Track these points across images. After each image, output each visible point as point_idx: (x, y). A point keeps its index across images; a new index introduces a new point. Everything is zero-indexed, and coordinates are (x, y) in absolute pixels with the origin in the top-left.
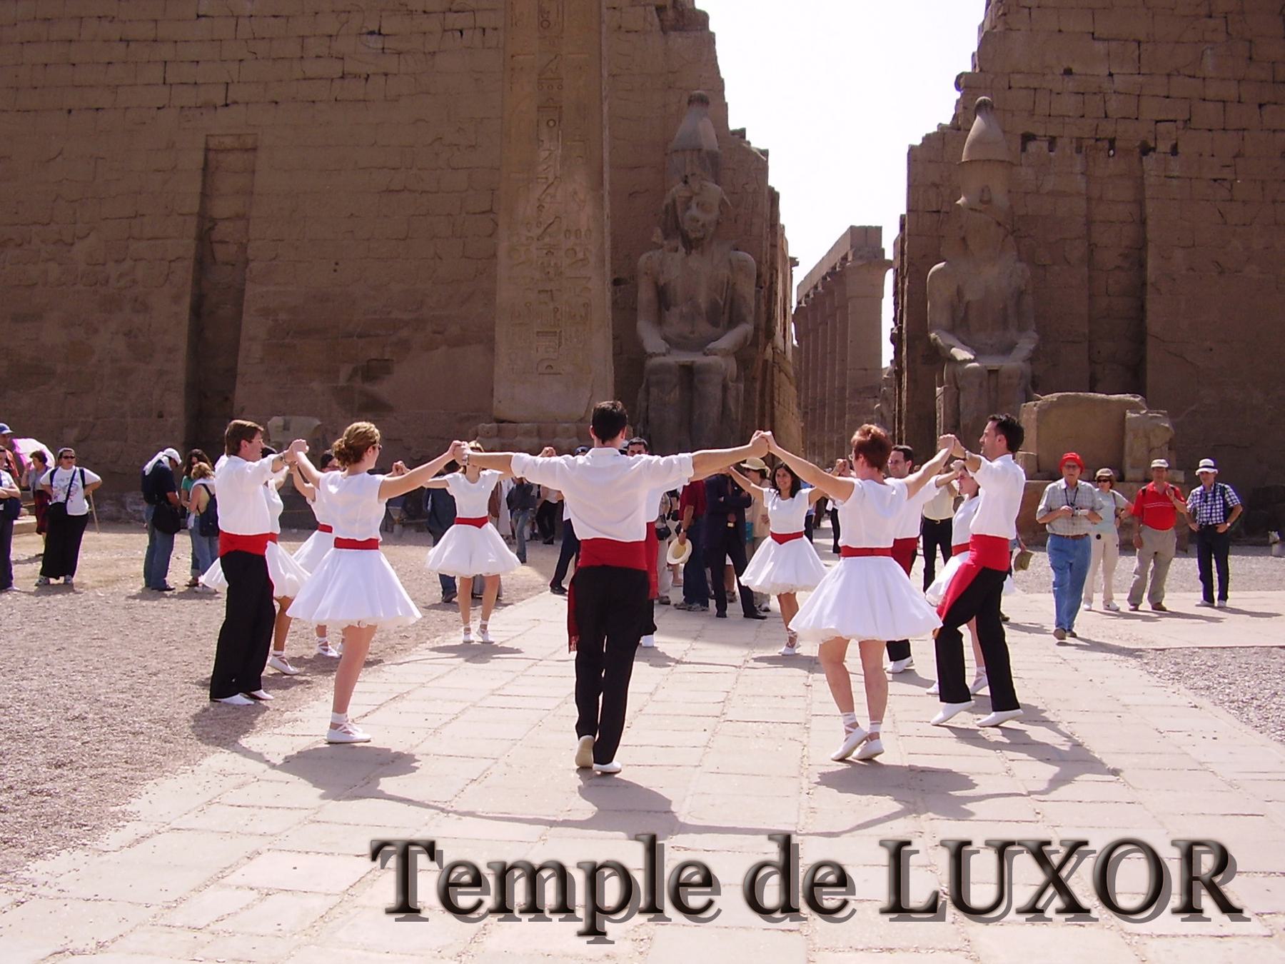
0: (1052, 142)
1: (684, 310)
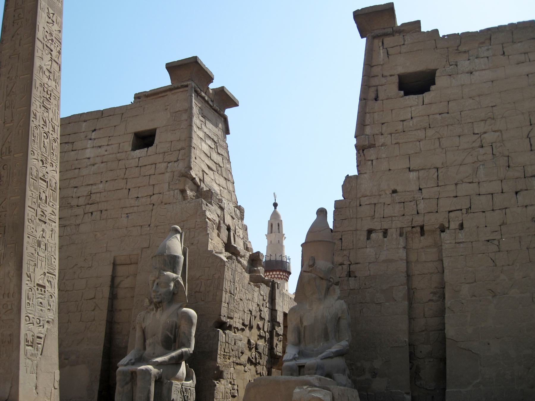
0: (385, 233)
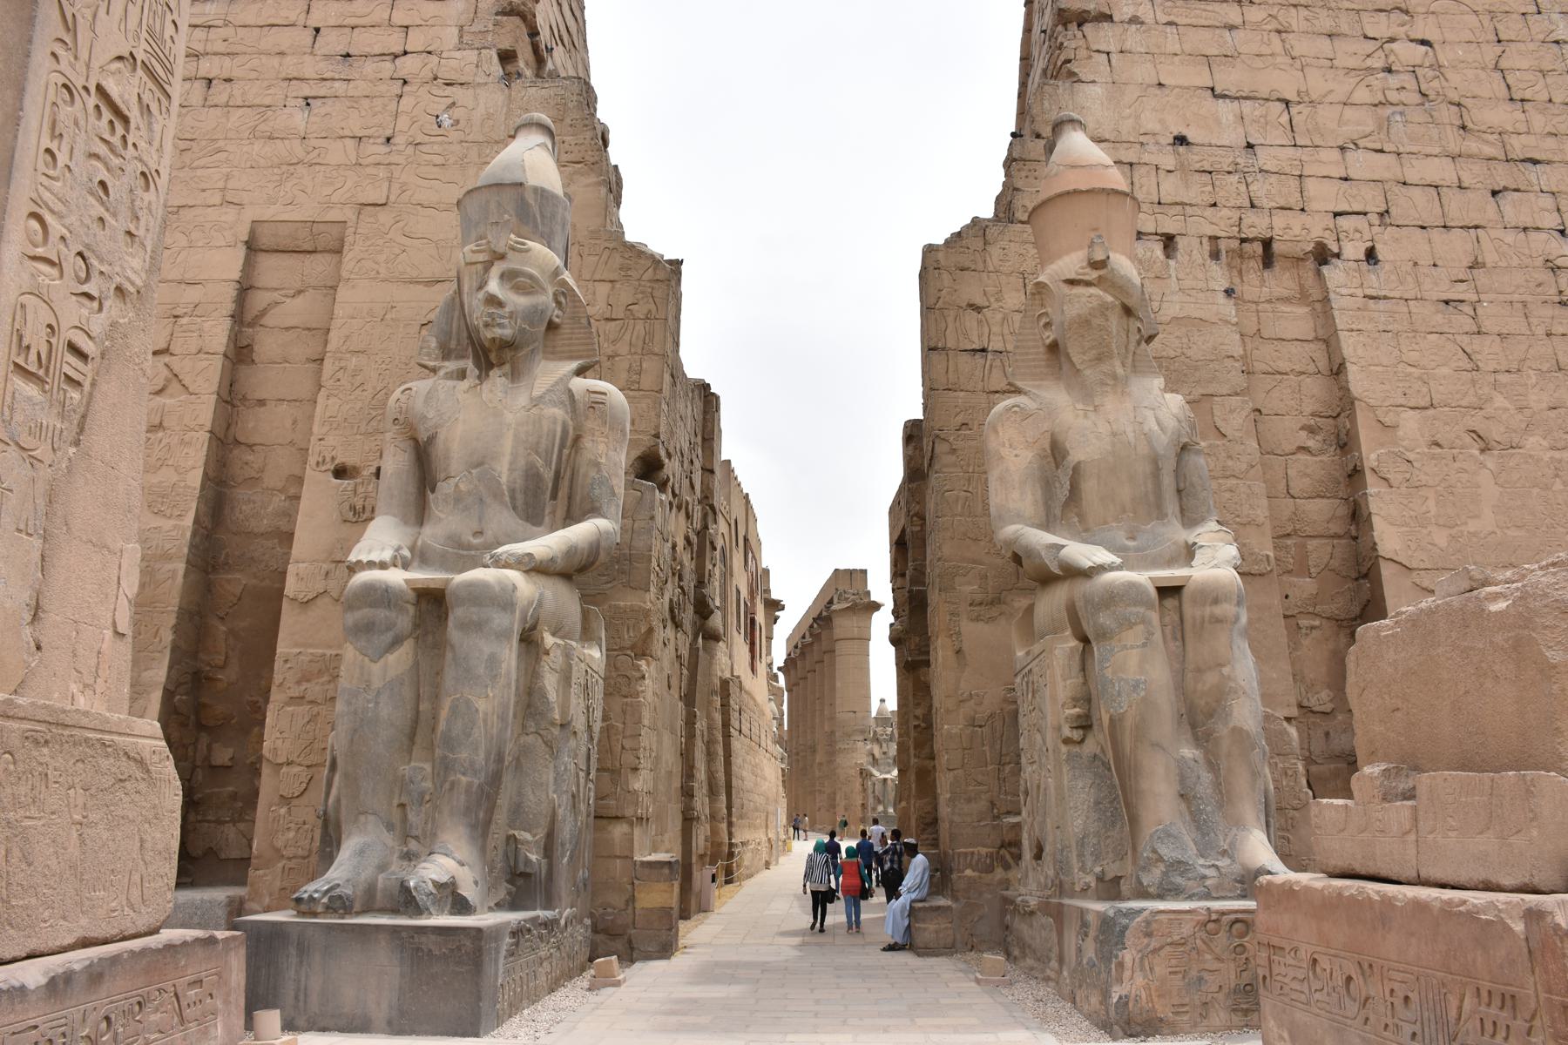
0: (1169, 241)
1: (462, 487)
